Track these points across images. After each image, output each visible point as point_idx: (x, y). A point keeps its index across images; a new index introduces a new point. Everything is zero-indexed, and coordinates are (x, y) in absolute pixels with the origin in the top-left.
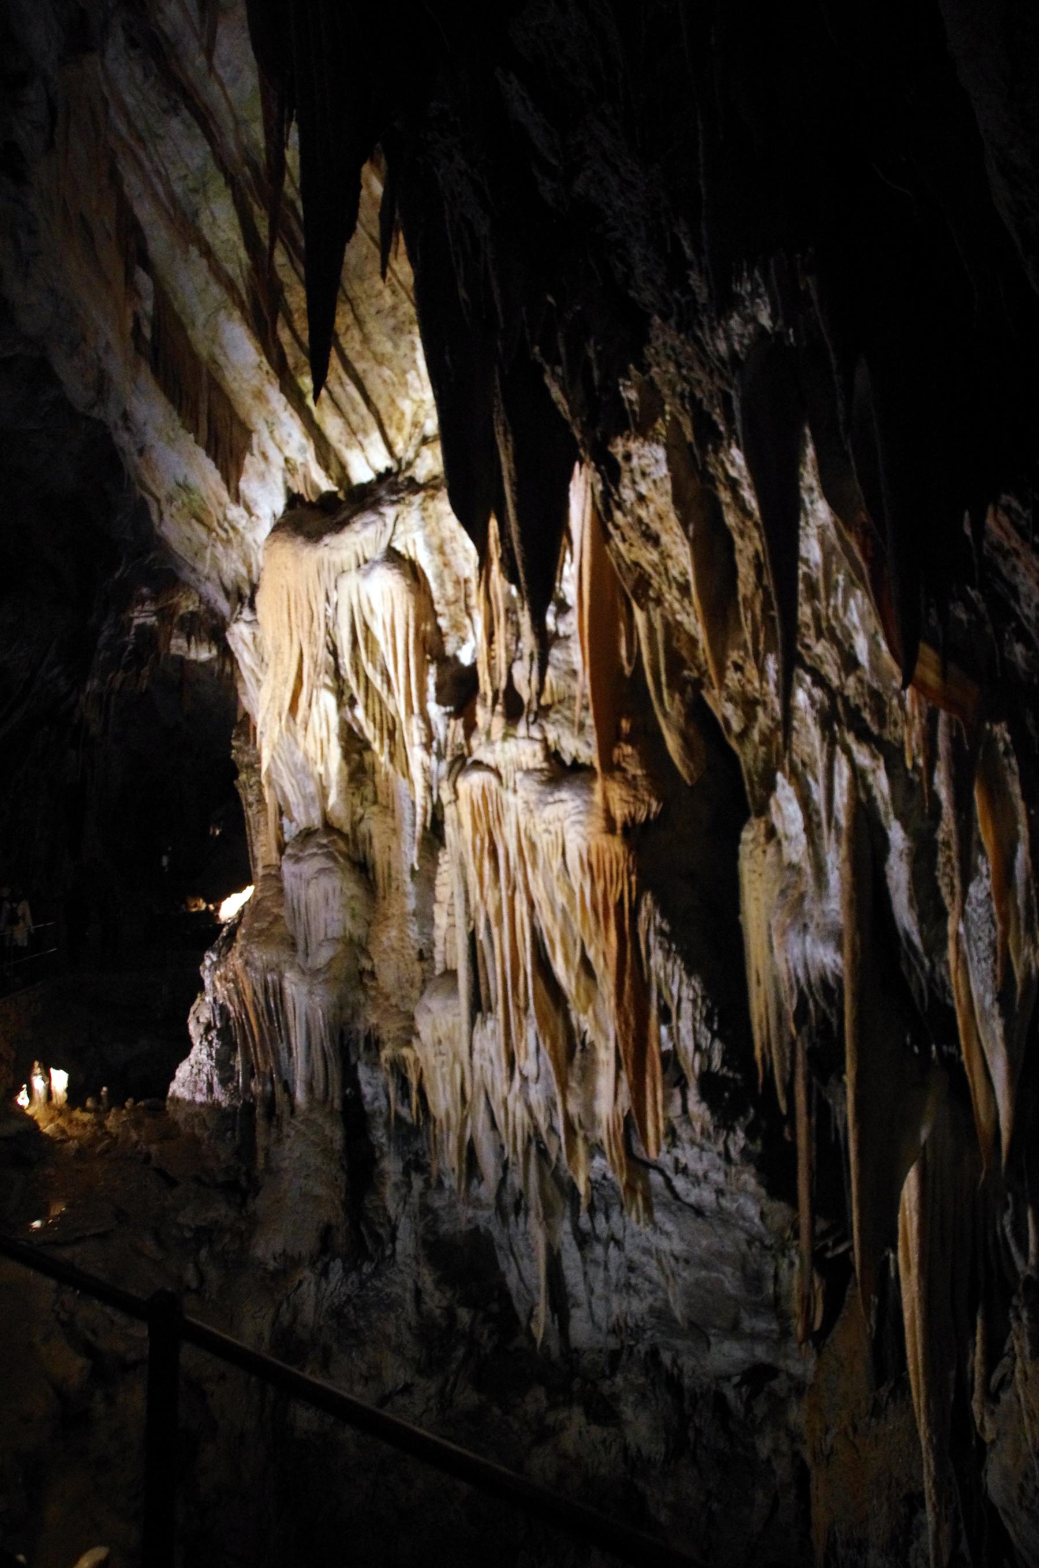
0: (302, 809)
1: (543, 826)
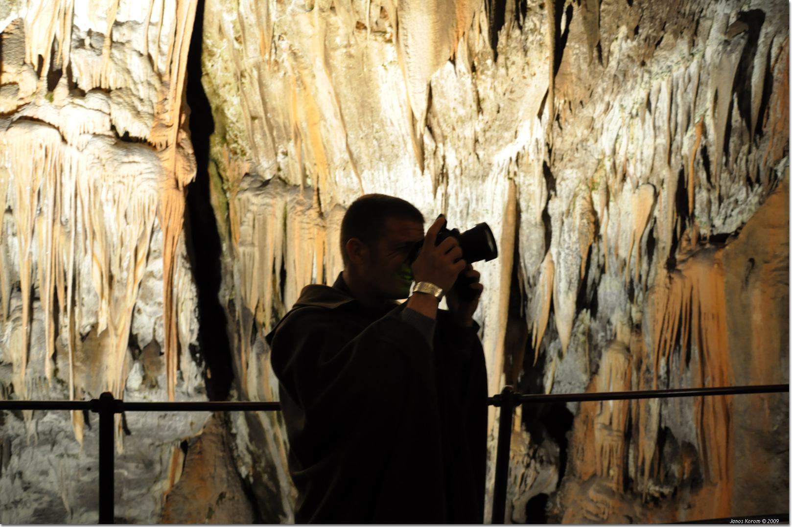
1: (118, 179)
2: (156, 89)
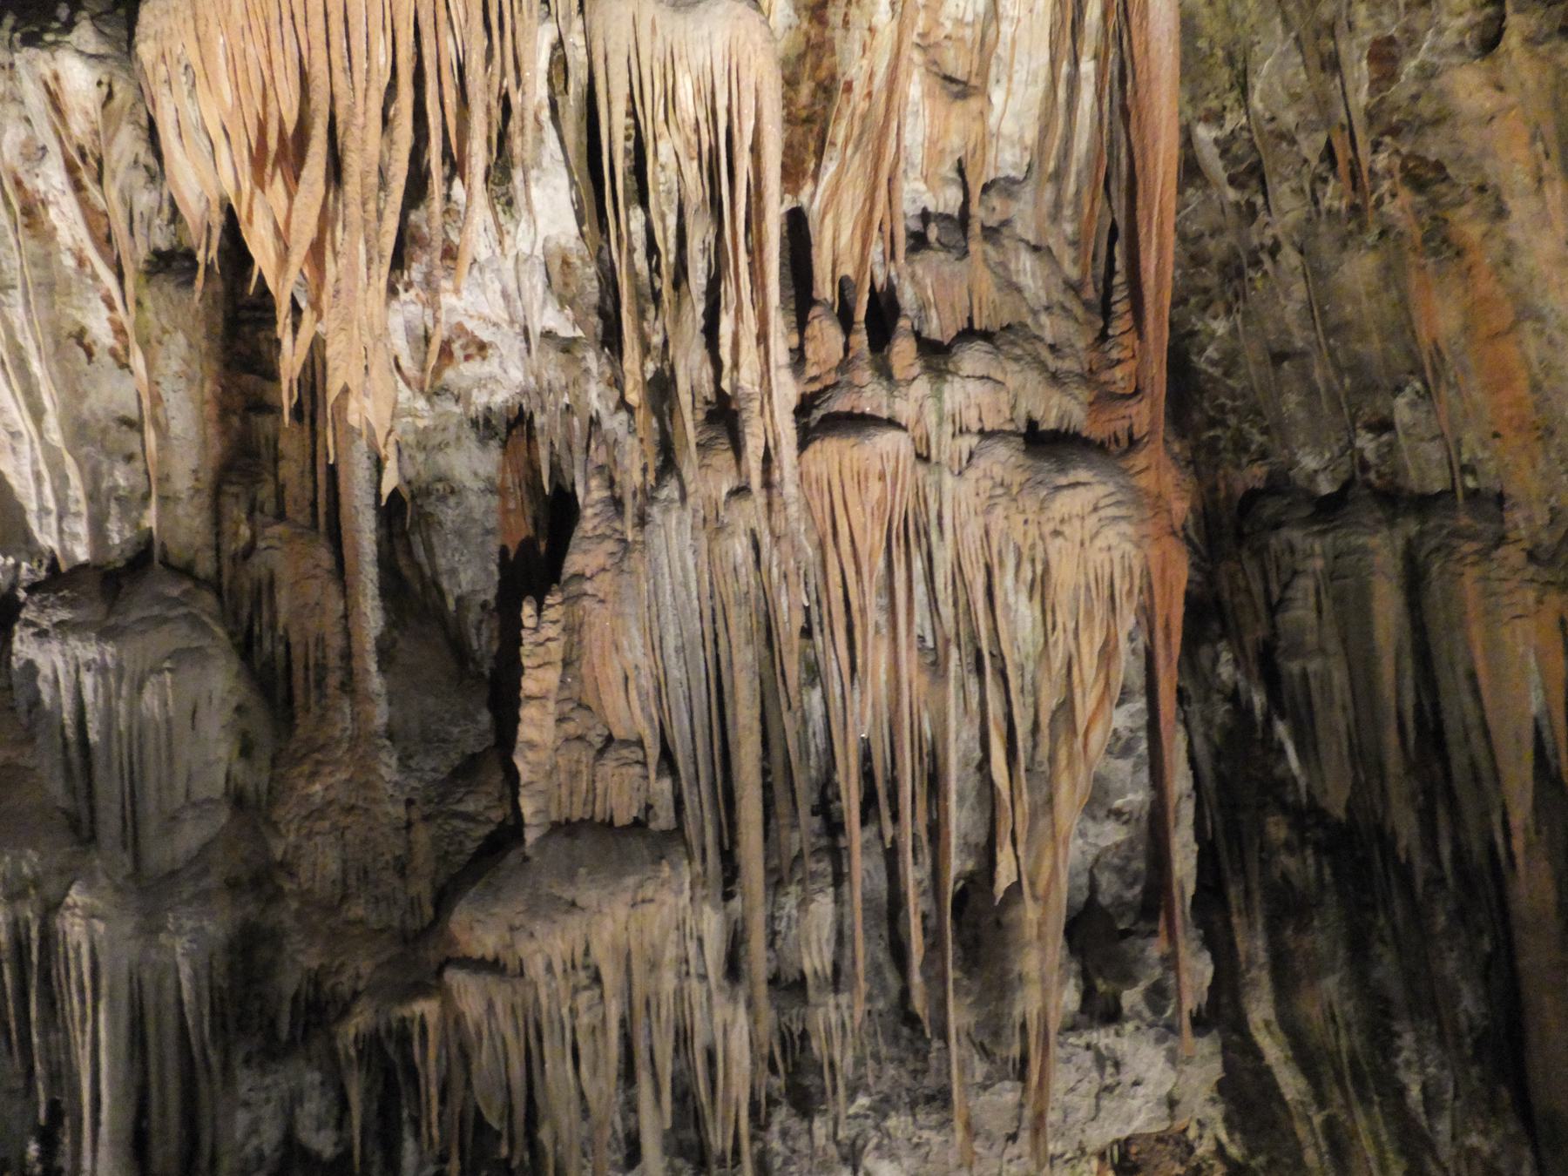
0: (82, 528)
2: (1076, 320)
